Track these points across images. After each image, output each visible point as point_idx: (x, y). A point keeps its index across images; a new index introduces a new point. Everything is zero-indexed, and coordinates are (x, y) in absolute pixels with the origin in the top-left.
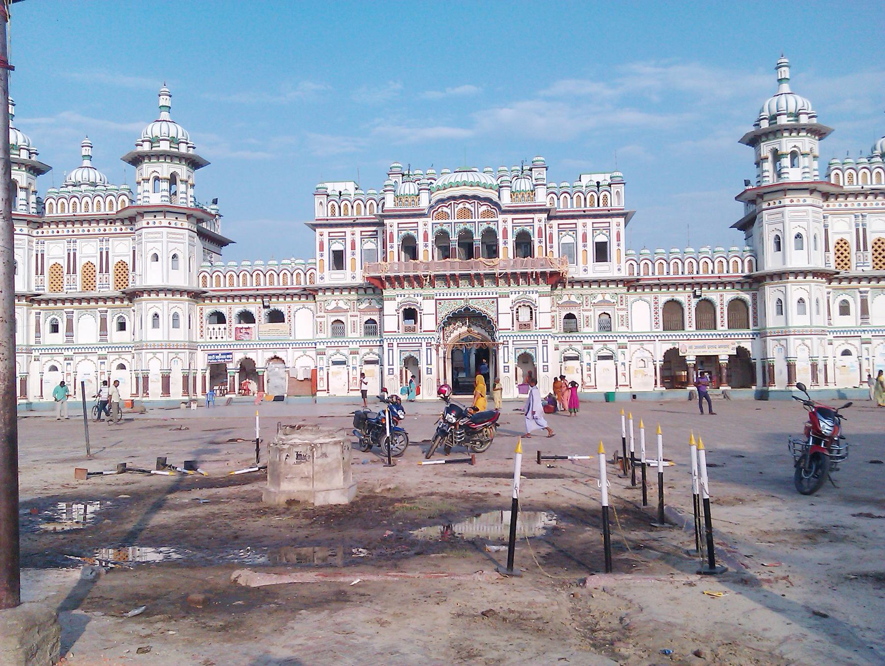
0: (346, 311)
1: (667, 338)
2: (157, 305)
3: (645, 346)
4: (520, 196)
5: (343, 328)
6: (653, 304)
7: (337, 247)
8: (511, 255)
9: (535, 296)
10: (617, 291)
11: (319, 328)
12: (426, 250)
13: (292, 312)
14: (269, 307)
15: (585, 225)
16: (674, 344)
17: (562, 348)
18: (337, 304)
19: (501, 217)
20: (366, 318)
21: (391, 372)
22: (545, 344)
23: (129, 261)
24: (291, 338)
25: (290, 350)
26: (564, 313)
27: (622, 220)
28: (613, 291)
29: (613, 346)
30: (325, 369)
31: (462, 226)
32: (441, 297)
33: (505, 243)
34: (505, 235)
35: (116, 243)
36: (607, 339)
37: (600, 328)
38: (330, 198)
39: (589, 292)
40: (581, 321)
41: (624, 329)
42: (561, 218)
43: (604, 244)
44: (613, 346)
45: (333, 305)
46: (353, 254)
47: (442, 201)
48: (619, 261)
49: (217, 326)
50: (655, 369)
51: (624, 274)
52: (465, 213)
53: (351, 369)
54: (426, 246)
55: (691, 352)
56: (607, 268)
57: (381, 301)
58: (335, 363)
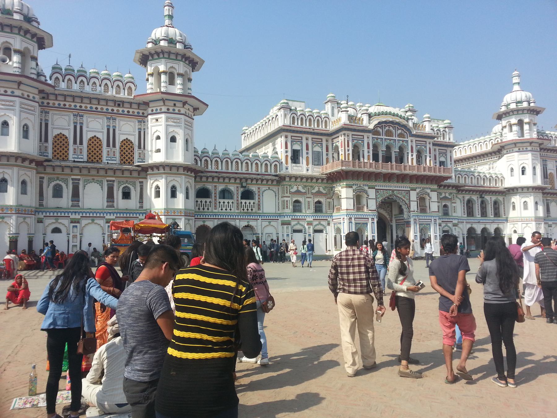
0: (305, 193)
2: (176, 179)
5: (300, 206)
6: (462, 200)
7: (297, 147)
8: (415, 163)
9: (429, 191)
10: (452, 191)
11: (285, 205)
14: (246, 187)
18: (298, 188)
19: (410, 139)
20: (316, 200)
23: (134, 139)
24: (261, 212)
25: (259, 221)
28: (450, 191)
29: (450, 225)
30: (290, 235)
32: (379, 188)
33: (412, 155)
34: (412, 152)
35: (122, 123)
44: (450, 225)
45: (295, 189)
47: (379, 123)
49: (204, 200)
50: (464, 239)
52: (389, 133)
53: (307, 235)
58: (295, 231)
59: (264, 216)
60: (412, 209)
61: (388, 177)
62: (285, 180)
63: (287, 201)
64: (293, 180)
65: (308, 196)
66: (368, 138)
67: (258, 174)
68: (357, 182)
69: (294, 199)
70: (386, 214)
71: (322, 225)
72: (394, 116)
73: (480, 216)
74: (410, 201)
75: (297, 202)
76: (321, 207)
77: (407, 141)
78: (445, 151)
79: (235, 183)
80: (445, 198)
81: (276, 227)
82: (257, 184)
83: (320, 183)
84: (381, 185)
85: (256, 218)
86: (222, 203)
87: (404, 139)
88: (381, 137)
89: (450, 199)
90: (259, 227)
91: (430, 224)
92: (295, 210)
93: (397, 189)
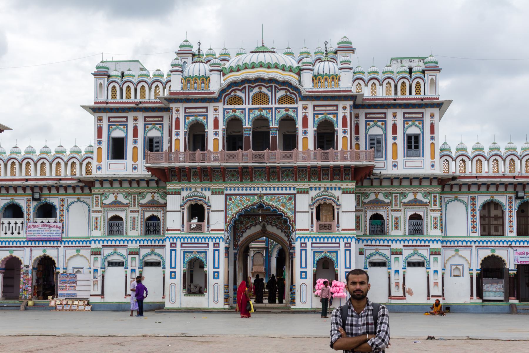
0: (127, 205)
1: (485, 244)
3: (461, 253)
4: (323, 81)
5: (122, 225)
7: (118, 133)
8: (311, 146)
9: (337, 193)
10: (430, 190)
12: (215, 139)
13: (65, 206)
14: (39, 199)
15: (395, 115)
16: (493, 251)
17: (368, 252)
18: (116, 197)
19: (300, 104)
20: (148, 214)
21: (173, 275)
22: (348, 249)
25: (61, 249)
26: (370, 214)
27: (436, 111)
28: (425, 190)
31: (257, 112)
32: (232, 192)
33: (305, 132)
36: (419, 243)
37: (410, 230)
38: (111, 79)
39: (399, 190)
40: (390, 223)
41: (437, 233)
42: (370, 106)
43: (417, 137)
44: (424, 252)
45: (111, 199)
46: (135, 142)
48: (433, 157)
50: (472, 278)
51: (438, 171)
52: (260, 98)
53: (129, 271)
54: (216, 134)
55: (511, 261)
56: (419, 164)
57: (164, 195)
58: (112, 264)
59: (68, 242)
60: (298, 226)
61: (245, 174)
62: (94, 186)
63: (97, 219)
64: (107, 185)
65: (133, 208)
66: (216, 110)
67: (60, 180)
68: (188, 186)
69: (110, 215)
70: (282, 235)
71: (156, 254)
72: (269, 67)
73: (515, 233)
74: (295, 212)
75: (116, 218)
76: (159, 226)
77: (297, 108)
78: (420, 115)
79: (25, 194)
80: (415, 202)
81: (88, 258)
82: (58, 194)
83: (153, 188)
84: (234, 187)
85: (56, 244)
86: (6, 225)
87: (289, 106)
88: (243, 106)
89: (425, 205)
90: (61, 259)
91: (337, 252)
92: (111, 232)
93: (268, 192)
